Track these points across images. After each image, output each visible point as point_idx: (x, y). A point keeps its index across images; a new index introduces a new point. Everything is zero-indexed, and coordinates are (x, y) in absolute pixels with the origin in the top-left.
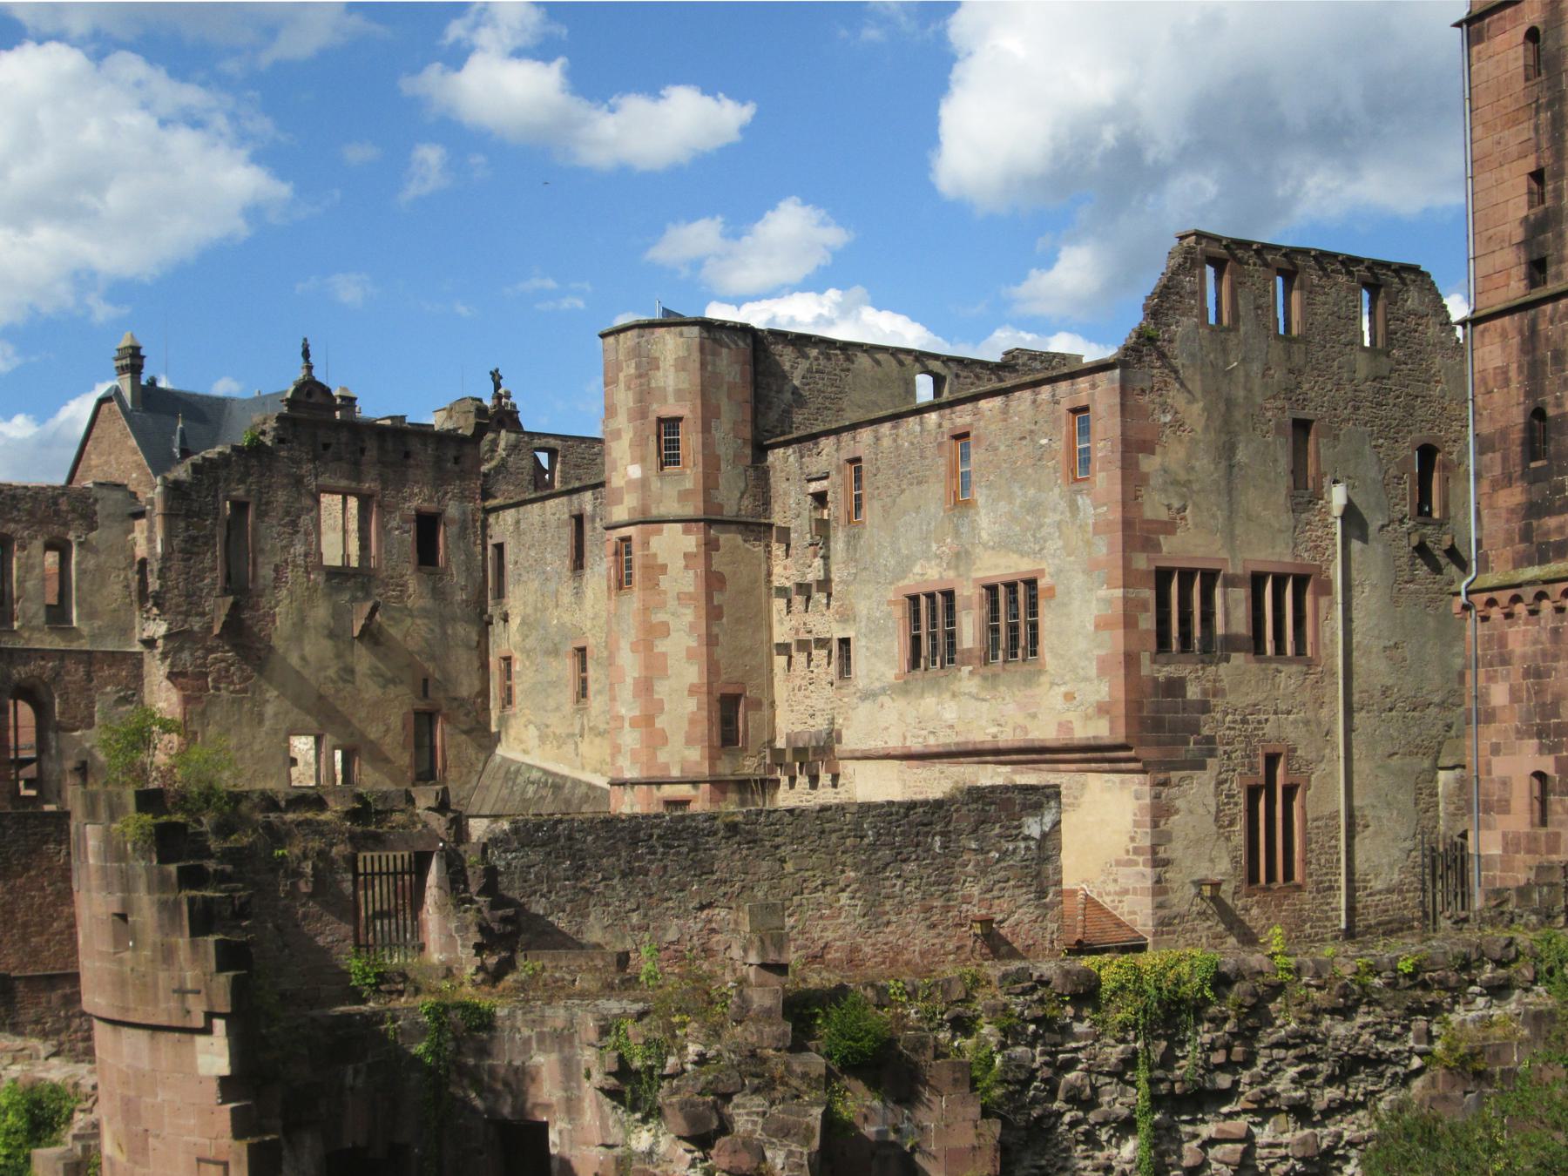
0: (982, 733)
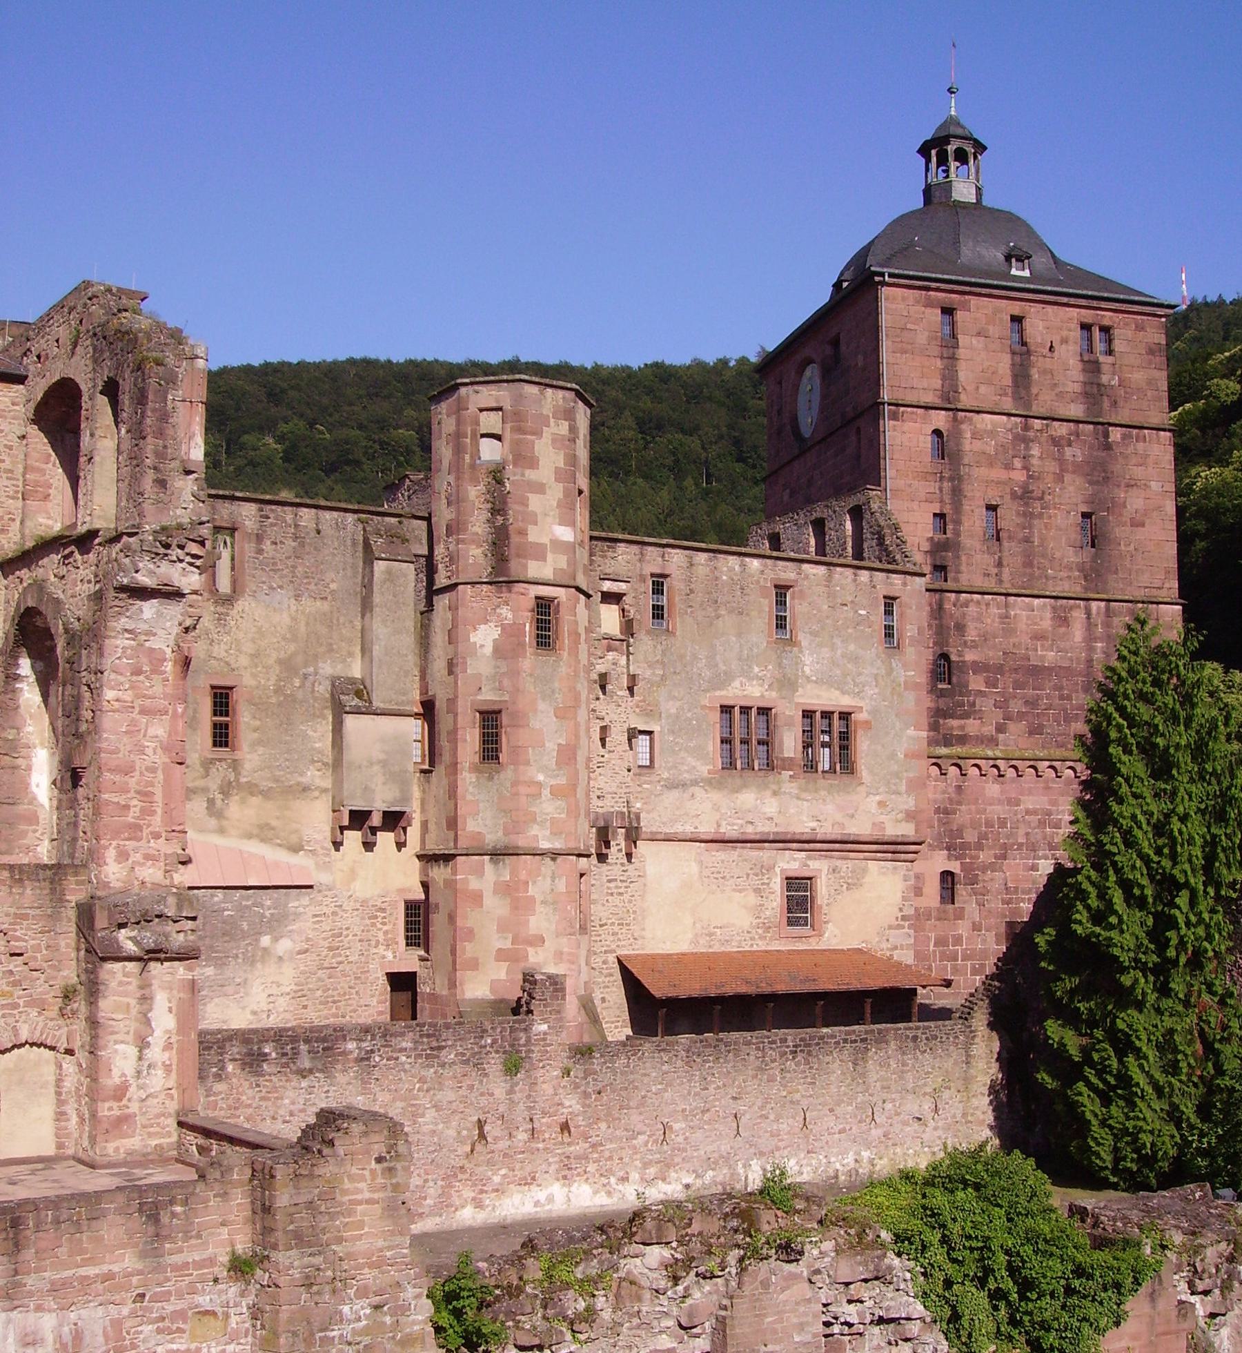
0: (803, 825)
